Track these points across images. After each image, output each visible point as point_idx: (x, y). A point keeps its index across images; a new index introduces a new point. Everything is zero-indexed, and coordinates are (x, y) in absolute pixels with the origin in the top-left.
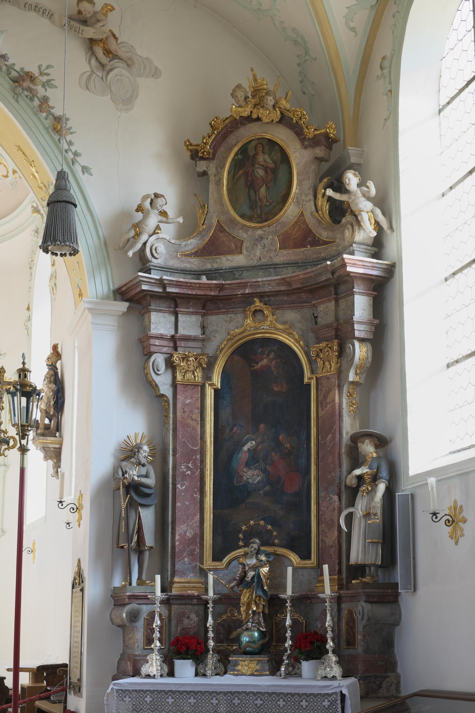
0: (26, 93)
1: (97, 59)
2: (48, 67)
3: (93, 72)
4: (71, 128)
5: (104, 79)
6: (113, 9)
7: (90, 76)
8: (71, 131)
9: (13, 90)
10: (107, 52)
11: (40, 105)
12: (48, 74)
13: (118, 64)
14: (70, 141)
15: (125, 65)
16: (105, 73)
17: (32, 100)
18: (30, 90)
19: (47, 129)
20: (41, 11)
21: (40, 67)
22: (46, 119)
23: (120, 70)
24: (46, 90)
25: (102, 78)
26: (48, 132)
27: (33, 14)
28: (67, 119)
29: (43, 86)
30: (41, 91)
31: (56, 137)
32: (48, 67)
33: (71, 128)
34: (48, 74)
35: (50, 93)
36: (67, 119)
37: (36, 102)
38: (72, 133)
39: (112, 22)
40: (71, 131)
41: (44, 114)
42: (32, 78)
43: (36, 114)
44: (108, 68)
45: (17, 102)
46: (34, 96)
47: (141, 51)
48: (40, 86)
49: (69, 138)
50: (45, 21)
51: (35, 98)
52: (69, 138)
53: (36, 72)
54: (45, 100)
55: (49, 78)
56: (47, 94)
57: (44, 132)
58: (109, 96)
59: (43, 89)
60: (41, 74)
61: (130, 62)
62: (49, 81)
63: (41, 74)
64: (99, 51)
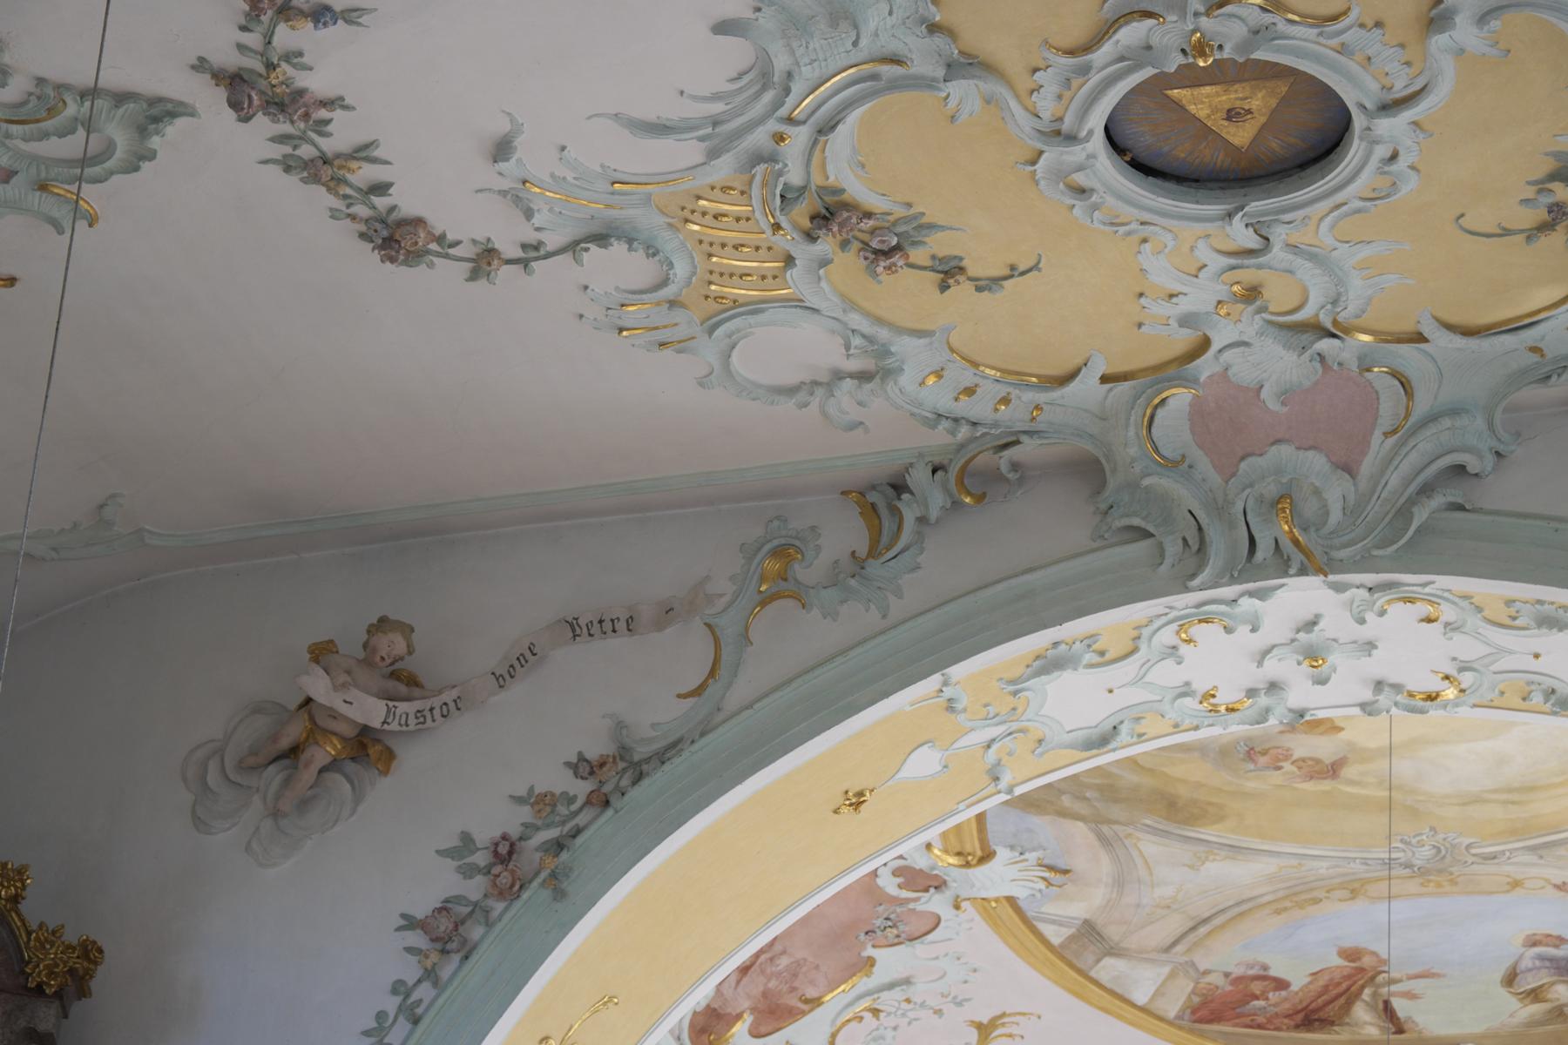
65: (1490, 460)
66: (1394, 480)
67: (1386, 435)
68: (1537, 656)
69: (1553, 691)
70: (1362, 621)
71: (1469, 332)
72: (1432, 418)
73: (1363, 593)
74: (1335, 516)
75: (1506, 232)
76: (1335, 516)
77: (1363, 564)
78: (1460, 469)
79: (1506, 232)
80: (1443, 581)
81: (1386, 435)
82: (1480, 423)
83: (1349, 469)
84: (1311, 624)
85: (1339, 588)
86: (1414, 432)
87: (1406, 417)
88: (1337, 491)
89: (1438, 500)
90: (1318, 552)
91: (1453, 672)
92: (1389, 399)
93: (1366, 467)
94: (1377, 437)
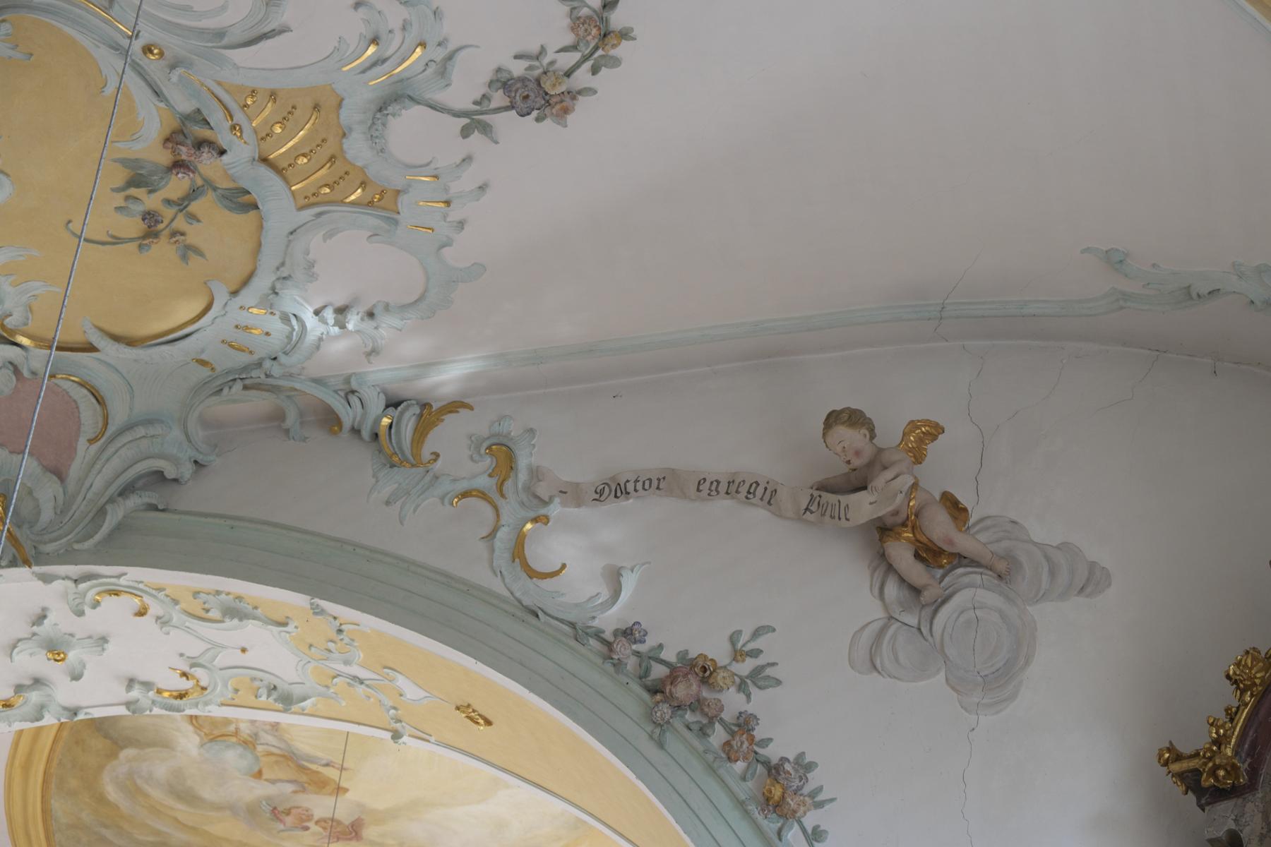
0: (689, 716)
1: (902, 580)
2: (756, 634)
3: (891, 617)
4: (820, 789)
5: (925, 630)
6: (934, 431)
7: (883, 631)
8: (820, 798)
9: (650, 716)
10: (929, 554)
11: (727, 743)
12: (755, 653)
13: (966, 580)
14: (815, 828)
15: (988, 578)
16: (927, 612)
17: (703, 732)
18: (698, 705)
19: (741, 805)
20: (744, 490)
21: (733, 639)
22: (744, 779)
23: (971, 595)
24: (748, 696)
25: (919, 629)
26: (746, 813)
27: (722, 505)
28: (810, 767)
29: (742, 687)
30: (732, 702)
31: (770, 825)
32: (756, 634)
33: (820, 789)
34: (755, 653)
35: (758, 702)
36: (810, 767)
37: (718, 736)
38: (820, 805)
39: (945, 469)
40: (820, 798)
41: (740, 766)
42: (704, 671)
43: (712, 770)
44: (927, 596)
45: (661, 745)
46: (711, 723)
47: (1043, 531)
48: (733, 690)
49: (811, 819)
50: (758, 514)
51: (717, 725)
52: (810, 820)
53: (718, 652)
54: (745, 724)
55: (760, 661)
56: (750, 708)
57: (734, 816)
58: (942, 675)
59: (742, 696)
60: (738, 655)
61: (1001, 566)
62: (758, 671)
63: (738, 655)
64: (901, 553)
65: (187, 470)
66: (98, 483)
67: (91, 441)
68: (244, 650)
69: (275, 688)
70: (80, 613)
71: (130, 342)
72: (129, 427)
73: (70, 584)
74: (47, 515)
75: (116, 241)
76: (47, 515)
77: (68, 557)
78: (159, 476)
79: (116, 241)
80: (134, 574)
81: (91, 441)
82: (176, 433)
83: (60, 475)
84: (41, 618)
85: (47, 579)
86: (112, 440)
87: (106, 424)
88: (49, 492)
89: (134, 501)
90: (28, 546)
91: (186, 669)
92: (88, 413)
93: (74, 471)
94: (82, 443)
